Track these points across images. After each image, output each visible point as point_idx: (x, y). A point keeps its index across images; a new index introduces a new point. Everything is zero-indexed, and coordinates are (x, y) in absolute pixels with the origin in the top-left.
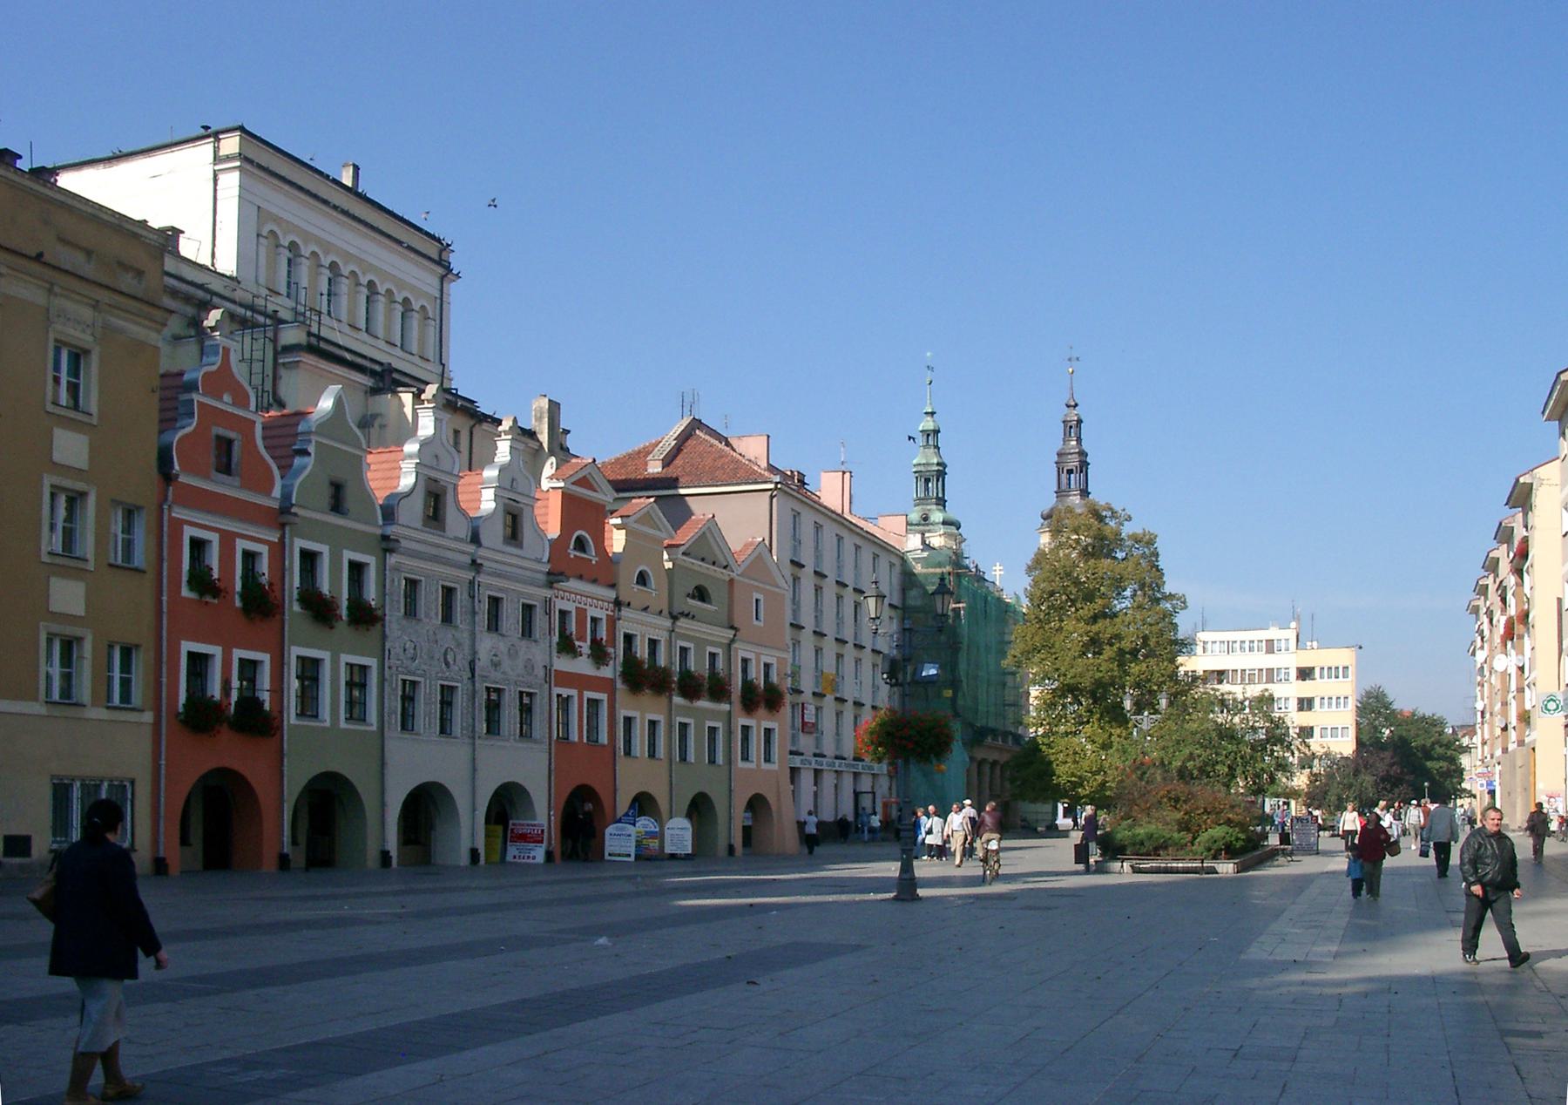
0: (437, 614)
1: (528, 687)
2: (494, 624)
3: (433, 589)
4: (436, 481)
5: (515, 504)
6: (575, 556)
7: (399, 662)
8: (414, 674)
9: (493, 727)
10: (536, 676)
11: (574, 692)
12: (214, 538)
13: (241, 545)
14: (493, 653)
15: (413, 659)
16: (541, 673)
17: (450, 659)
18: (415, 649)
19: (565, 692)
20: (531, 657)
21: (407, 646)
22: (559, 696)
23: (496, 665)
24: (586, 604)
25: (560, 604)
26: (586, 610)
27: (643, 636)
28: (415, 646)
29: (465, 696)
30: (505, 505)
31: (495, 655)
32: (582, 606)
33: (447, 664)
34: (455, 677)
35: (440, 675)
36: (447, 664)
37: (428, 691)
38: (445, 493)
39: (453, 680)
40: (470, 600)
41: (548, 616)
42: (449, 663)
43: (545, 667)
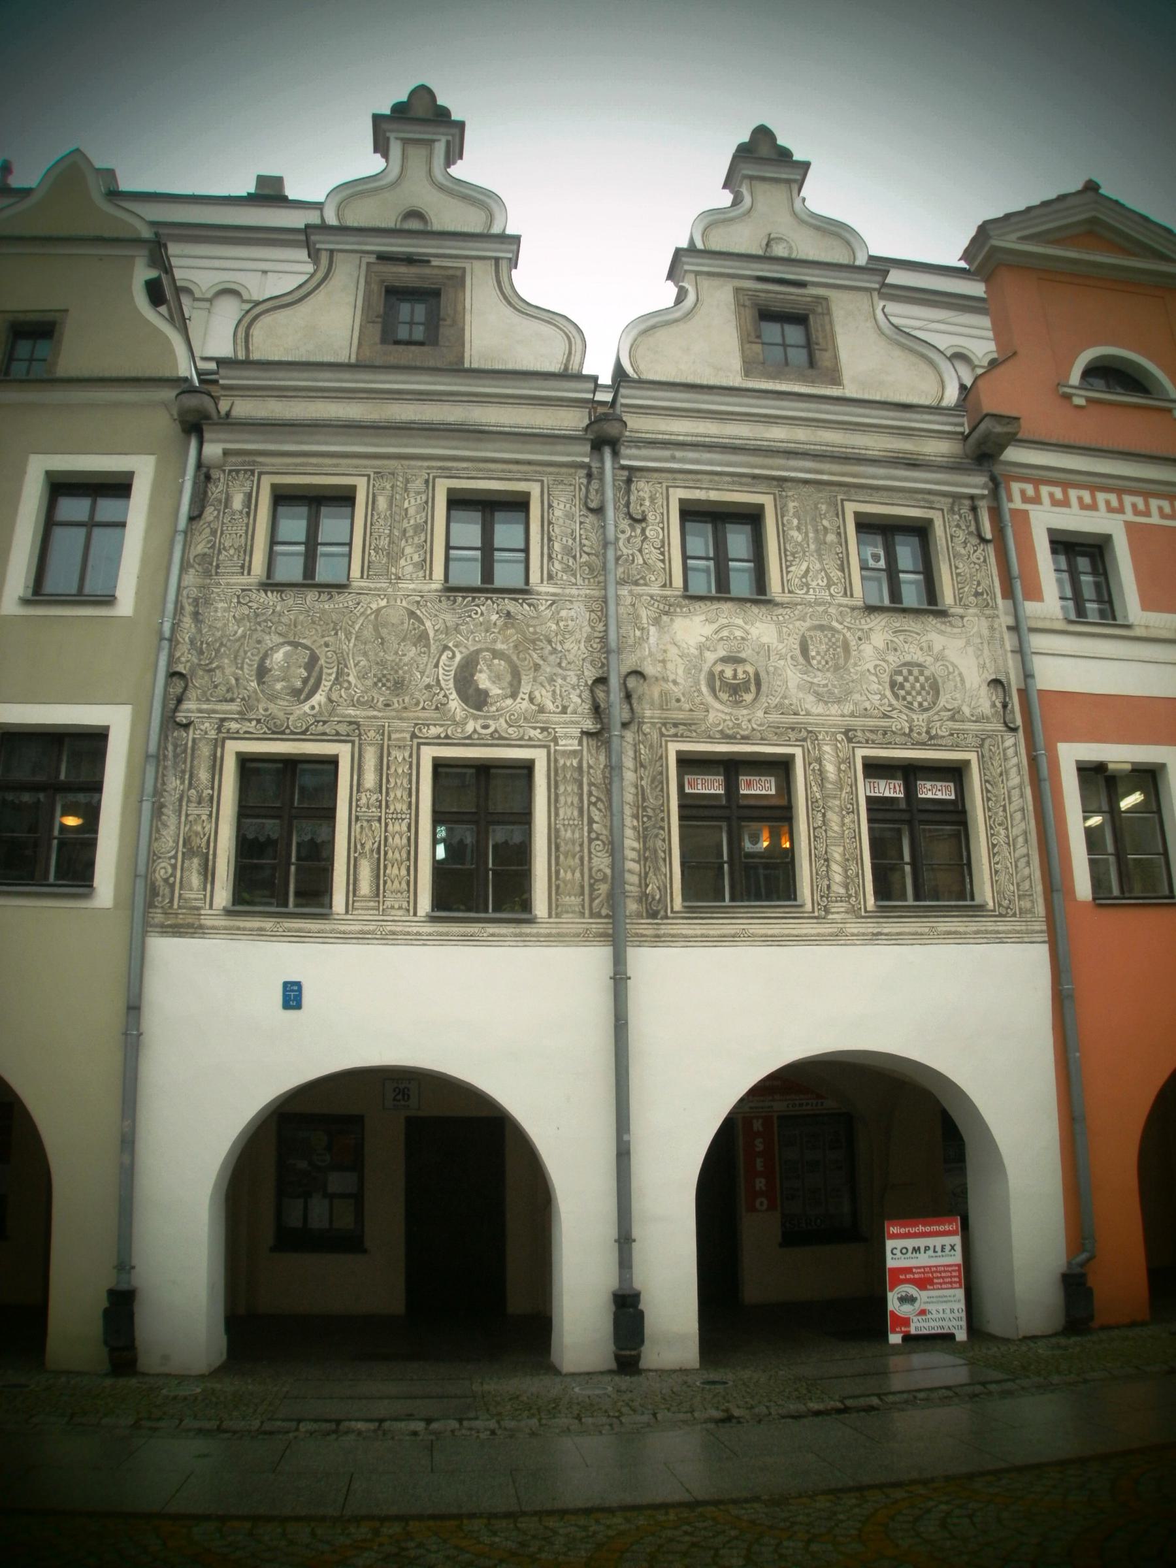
0: (425, 565)
1: (922, 745)
3: (411, 504)
4: (409, 260)
6: (1089, 400)
7: (233, 707)
8: (303, 735)
10: (957, 711)
14: (711, 657)
16: (985, 701)
17: (483, 680)
18: (312, 663)
20: (919, 657)
21: (279, 656)
28: (313, 659)
29: (567, 789)
30: (737, 290)
31: (732, 660)
33: (476, 699)
35: (434, 731)
36: (476, 699)
37: (370, 779)
38: (458, 280)
39: (498, 739)
40: (591, 519)
41: (990, 548)
42: (484, 694)
43: (996, 683)
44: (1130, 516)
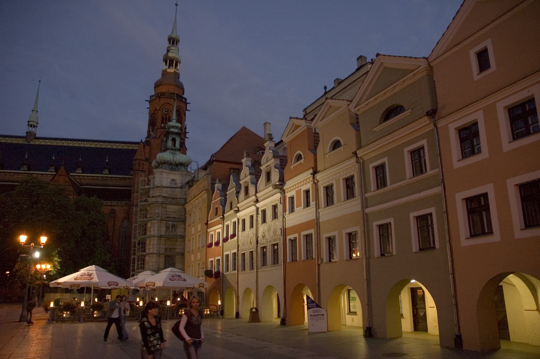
2: (264, 221)
5: (268, 167)
9: (264, 263)
11: (296, 235)
12: (213, 233)
13: (217, 231)
15: (244, 245)
17: (252, 242)
19: (292, 237)
20: (276, 227)
22: (290, 239)
23: (264, 237)
24: (300, 187)
25: (288, 195)
26: (301, 189)
27: (338, 181)
31: (264, 233)
32: (299, 188)
34: (252, 247)
44: (297, 189)
